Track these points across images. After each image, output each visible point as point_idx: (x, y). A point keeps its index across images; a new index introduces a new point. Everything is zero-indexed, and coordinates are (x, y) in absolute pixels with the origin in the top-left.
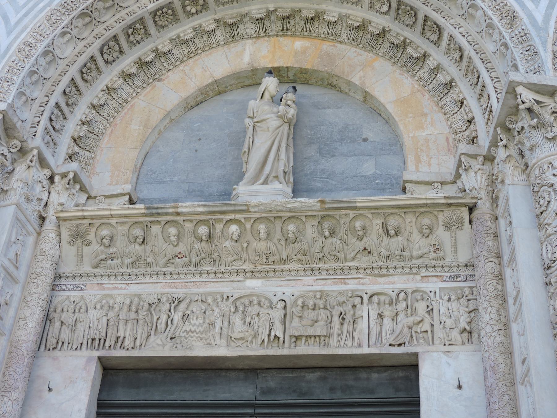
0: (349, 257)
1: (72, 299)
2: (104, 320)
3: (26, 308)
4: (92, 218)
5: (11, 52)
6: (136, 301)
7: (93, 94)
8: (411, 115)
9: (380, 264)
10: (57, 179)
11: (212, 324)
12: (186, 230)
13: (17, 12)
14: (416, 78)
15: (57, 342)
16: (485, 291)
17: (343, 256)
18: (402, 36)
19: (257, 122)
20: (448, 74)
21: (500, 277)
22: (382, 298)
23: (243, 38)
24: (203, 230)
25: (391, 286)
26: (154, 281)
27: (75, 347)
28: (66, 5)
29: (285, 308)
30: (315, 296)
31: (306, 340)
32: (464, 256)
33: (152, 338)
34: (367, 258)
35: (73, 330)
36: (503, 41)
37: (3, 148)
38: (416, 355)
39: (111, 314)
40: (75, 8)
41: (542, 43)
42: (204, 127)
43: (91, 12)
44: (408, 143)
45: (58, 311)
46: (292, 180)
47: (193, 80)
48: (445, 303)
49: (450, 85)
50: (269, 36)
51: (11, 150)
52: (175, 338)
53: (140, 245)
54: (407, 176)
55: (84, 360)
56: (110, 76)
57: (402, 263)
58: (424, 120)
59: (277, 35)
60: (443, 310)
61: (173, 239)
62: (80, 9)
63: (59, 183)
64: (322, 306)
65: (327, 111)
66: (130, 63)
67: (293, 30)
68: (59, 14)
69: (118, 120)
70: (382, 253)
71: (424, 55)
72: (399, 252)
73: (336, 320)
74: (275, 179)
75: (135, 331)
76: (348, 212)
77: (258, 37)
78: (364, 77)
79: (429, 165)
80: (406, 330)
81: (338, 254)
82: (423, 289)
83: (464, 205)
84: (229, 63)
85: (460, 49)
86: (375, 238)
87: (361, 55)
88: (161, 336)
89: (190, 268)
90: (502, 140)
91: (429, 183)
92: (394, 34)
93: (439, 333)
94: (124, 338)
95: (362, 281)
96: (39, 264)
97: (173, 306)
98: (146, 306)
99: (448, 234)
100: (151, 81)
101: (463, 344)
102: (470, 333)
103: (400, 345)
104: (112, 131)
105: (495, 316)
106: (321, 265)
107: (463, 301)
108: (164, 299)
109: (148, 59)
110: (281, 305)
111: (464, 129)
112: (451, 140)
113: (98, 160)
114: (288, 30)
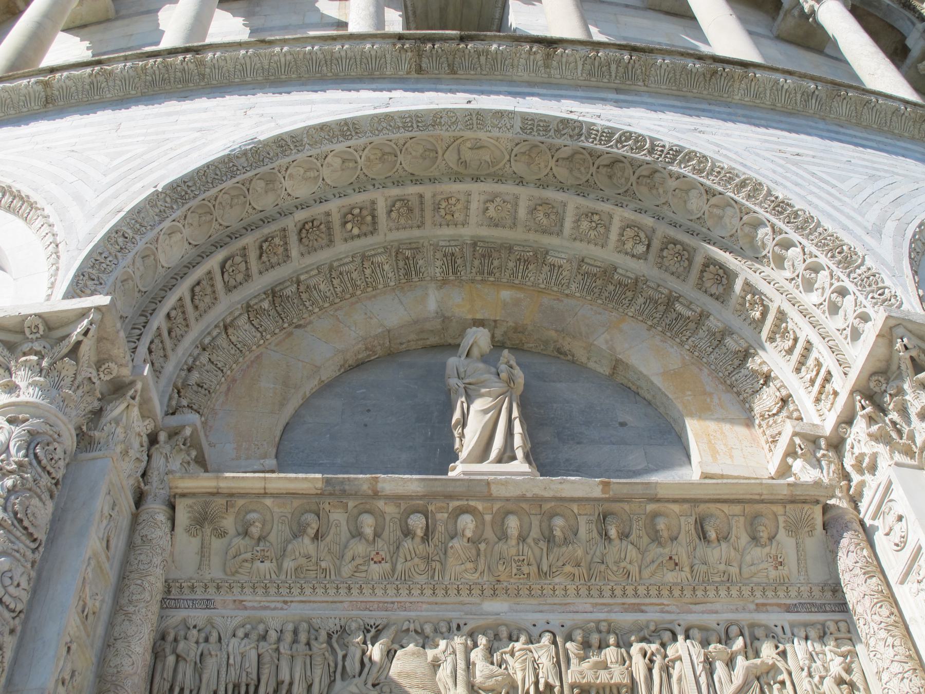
1: (191, 623)
2: (253, 655)
4: (232, 495)
6: (305, 626)
8: (689, 393)
10: (162, 437)
14: (687, 347)
16: (876, 617)
17: (637, 569)
19: (470, 384)
26: (331, 599)
28: (179, 189)
33: (339, 683)
35: (198, 670)
36: (836, 284)
37: (90, 370)
40: (192, 195)
43: (214, 206)
45: (170, 638)
47: (353, 328)
51: (102, 376)
52: (378, 684)
58: (708, 400)
59: (473, 281)
61: (369, 531)
62: (200, 198)
63: (165, 443)
65: (559, 385)
67: (497, 275)
68: (168, 199)
70: (696, 567)
72: (722, 567)
75: (309, 673)
77: (444, 282)
79: (731, 457)
81: (629, 567)
82: (763, 622)
84: (405, 310)
87: (600, 314)
88: (356, 680)
90: (863, 408)
92: (652, 285)
96: (142, 557)
100: (286, 325)
104: (229, 389)
109: (288, 292)
111: (774, 411)
113: (211, 427)
114: (490, 274)
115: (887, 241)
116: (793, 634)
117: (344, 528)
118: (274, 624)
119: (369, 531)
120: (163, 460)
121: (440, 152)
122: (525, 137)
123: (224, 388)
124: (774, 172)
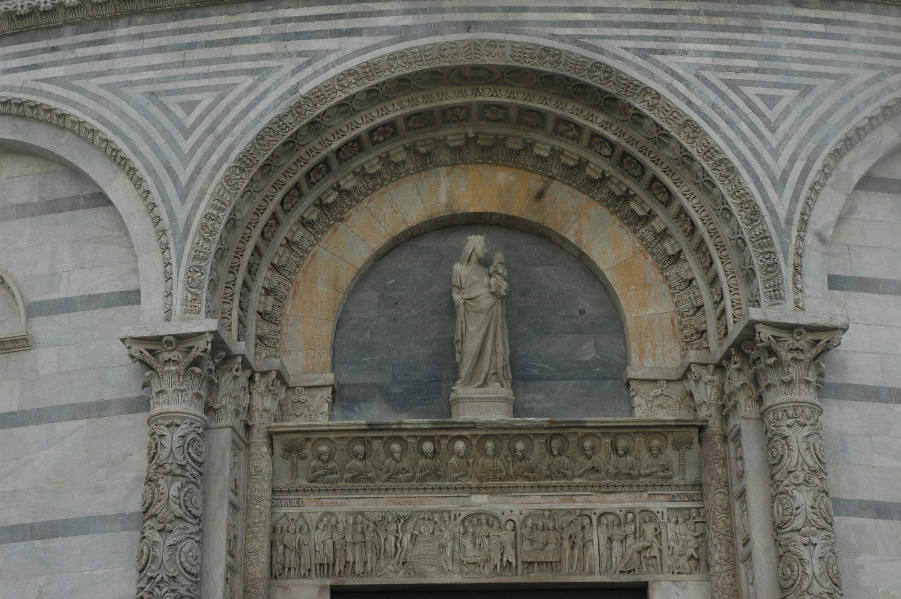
0: (576, 473)
1: (290, 517)
2: (330, 542)
3: (254, 540)
4: (308, 432)
5: (194, 229)
7: (275, 252)
8: (633, 287)
9: (608, 481)
10: (257, 377)
11: (443, 547)
12: (409, 445)
13: (185, 166)
15: (283, 568)
16: (714, 527)
18: (625, 185)
20: (676, 243)
21: (728, 510)
22: (611, 518)
23: (436, 166)
24: (428, 446)
25: (619, 506)
27: (303, 573)
29: (514, 529)
30: (543, 514)
31: (539, 565)
32: (691, 476)
34: (595, 476)
35: (299, 555)
38: (646, 583)
39: (336, 537)
41: (784, 253)
42: (399, 286)
44: (630, 325)
45: (279, 531)
46: (510, 377)
48: (671, 526)
49: (676, 258)
50: (466, 163)
53: (361, 460)
54: (629, 376)
55: (316, 590)
56: (289, 228)
57: (630, 481)
59: (475, 163)
60: (671, 535)
61: (397, 455)
64: (551, 528)
65: (540, 270)
66: (310, 206)
69: (300, 277)
71: (650, 212)
73: (567, 544)
74: (494, 377)
76: (578, 430)
77: (454, 164)
78: (580, 231)
79: (654, 355)
80: (635, 555)
83: (695, 426)
85: (692, 224)
86: (603, 456)
89: (413, 483)
90: (736, 363)
91: (655, 381)
93: (668, 561)
94: (354, 562)
95: (589, 498)
96: (257, 485)
97: (400, 525)
98: (372, 525)
99: (676, 453)
101: (691, 573)
102: (698, 560)
103: (629, 572)
104: (295, 293)
105: (724, 555)
106: (548, 482)
107: (691, 522)
108: (390, 518)
109: (330, 200)
110: (510, 526)
111: (692, 312)
112: (676, 323)
114: (489, 158)
115: (788, 192)
116: (668, 519)
117: (382, 451)
118: (341, 517)
119: (397, 455)
120: (260, 398)
121: (445, 75)
122: (513, 63)
123: (291, 292)
124: (714, 106)
